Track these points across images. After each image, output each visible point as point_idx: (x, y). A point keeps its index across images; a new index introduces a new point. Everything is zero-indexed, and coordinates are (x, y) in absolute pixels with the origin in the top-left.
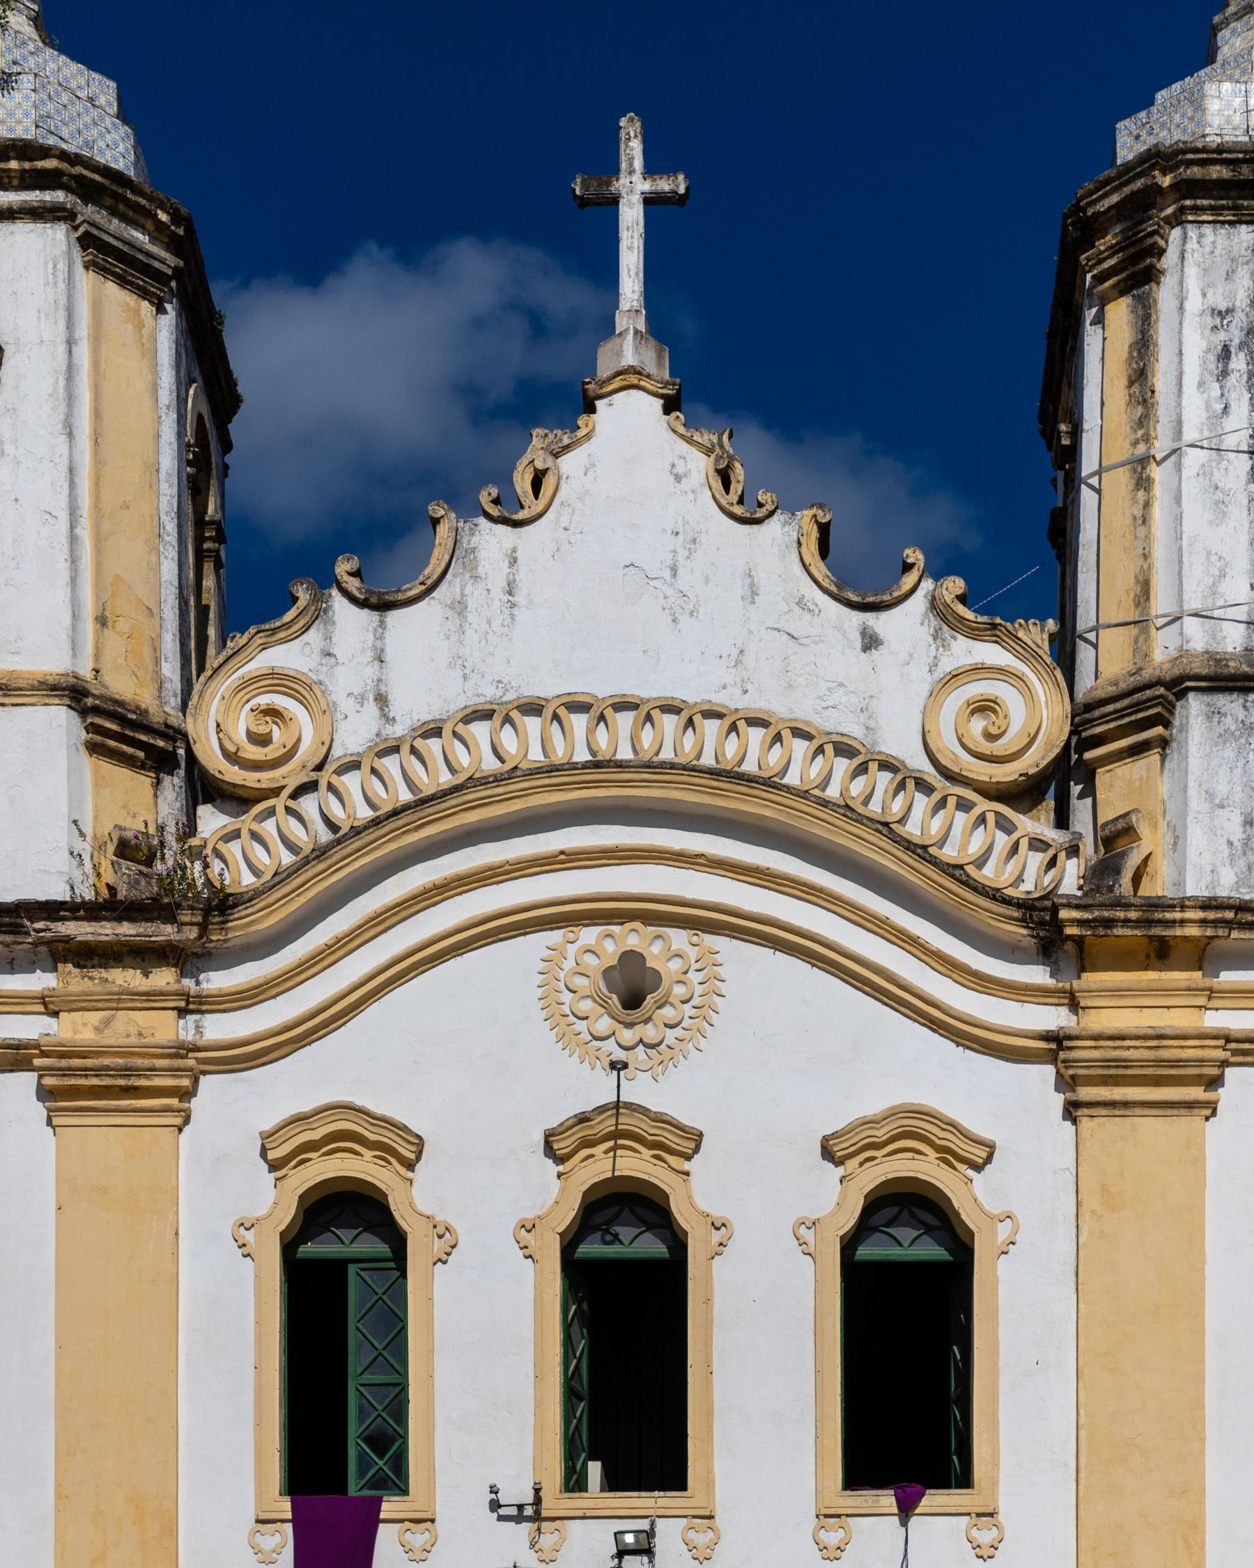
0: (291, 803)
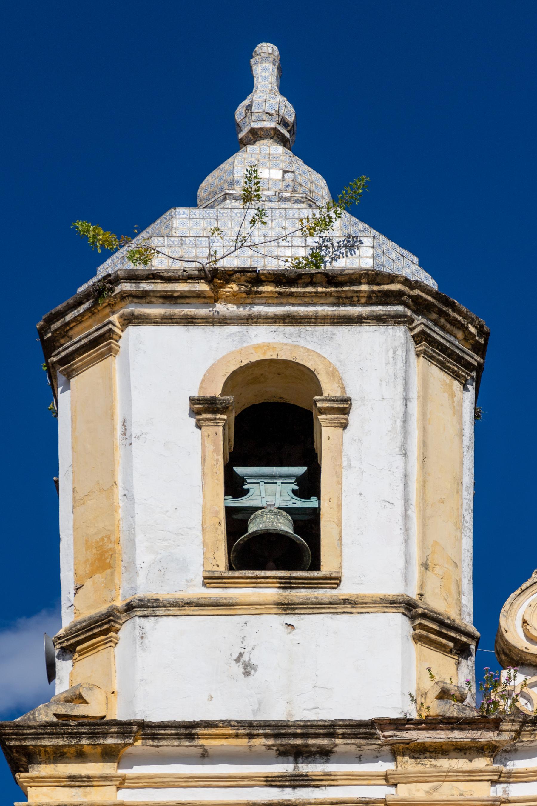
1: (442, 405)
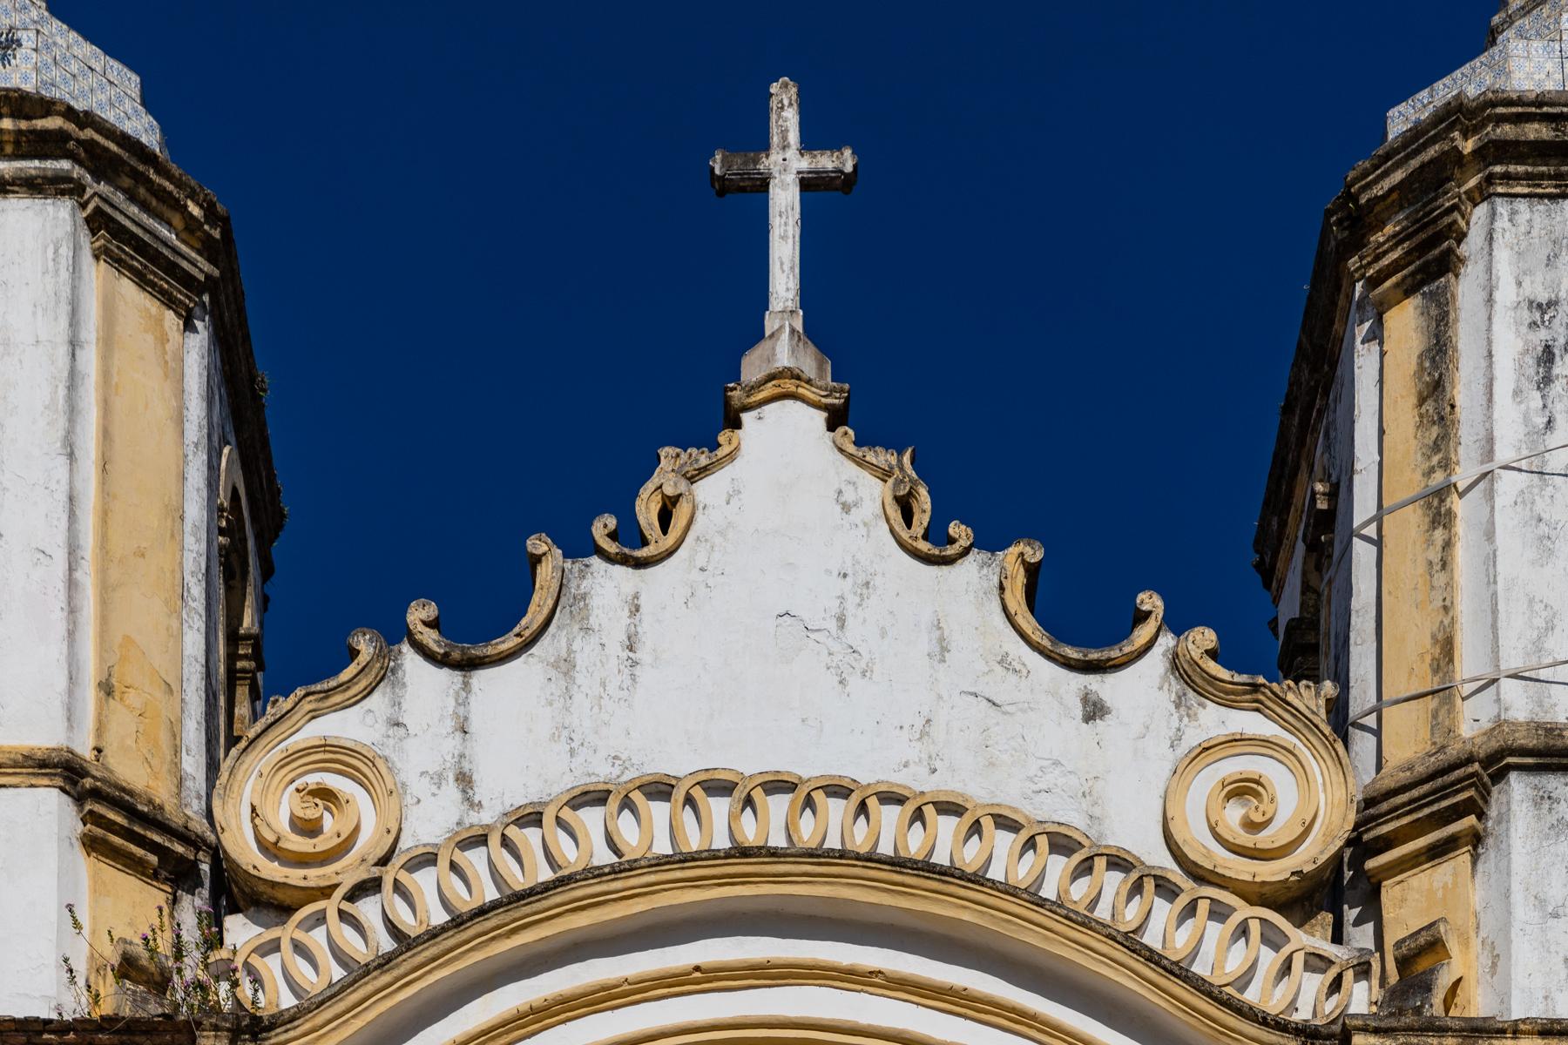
0: (346, 906)
1: (142, 358)
